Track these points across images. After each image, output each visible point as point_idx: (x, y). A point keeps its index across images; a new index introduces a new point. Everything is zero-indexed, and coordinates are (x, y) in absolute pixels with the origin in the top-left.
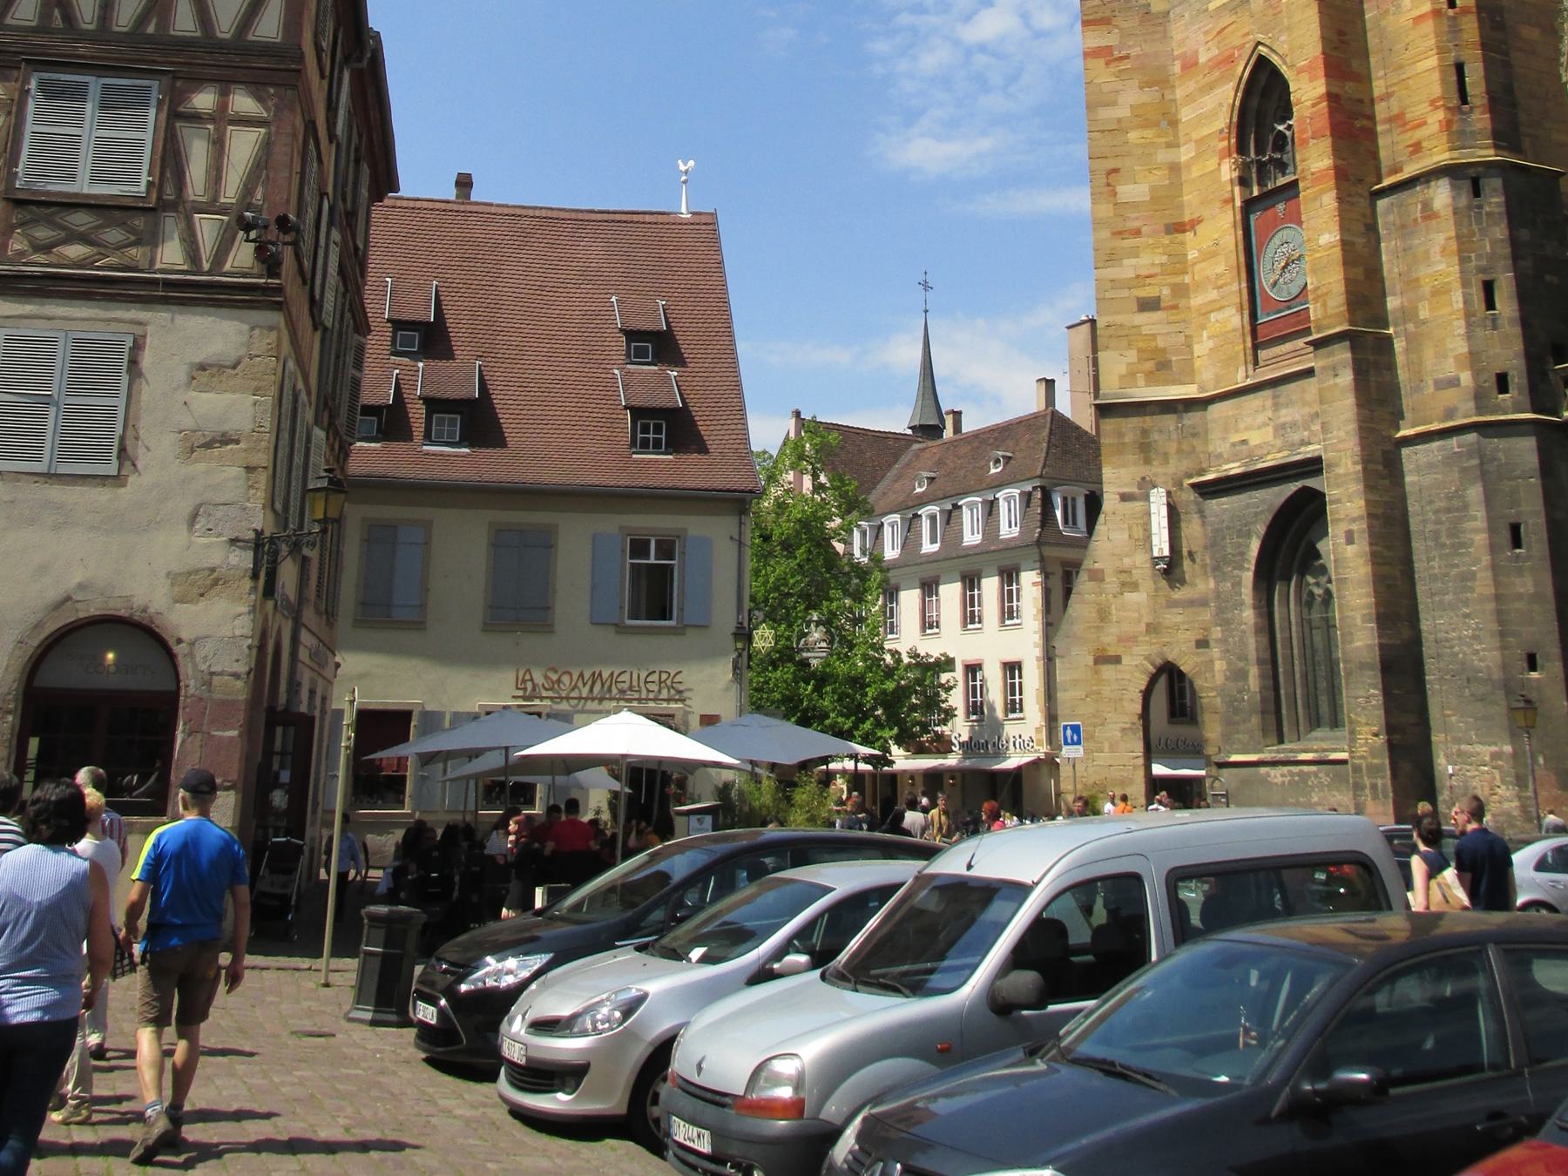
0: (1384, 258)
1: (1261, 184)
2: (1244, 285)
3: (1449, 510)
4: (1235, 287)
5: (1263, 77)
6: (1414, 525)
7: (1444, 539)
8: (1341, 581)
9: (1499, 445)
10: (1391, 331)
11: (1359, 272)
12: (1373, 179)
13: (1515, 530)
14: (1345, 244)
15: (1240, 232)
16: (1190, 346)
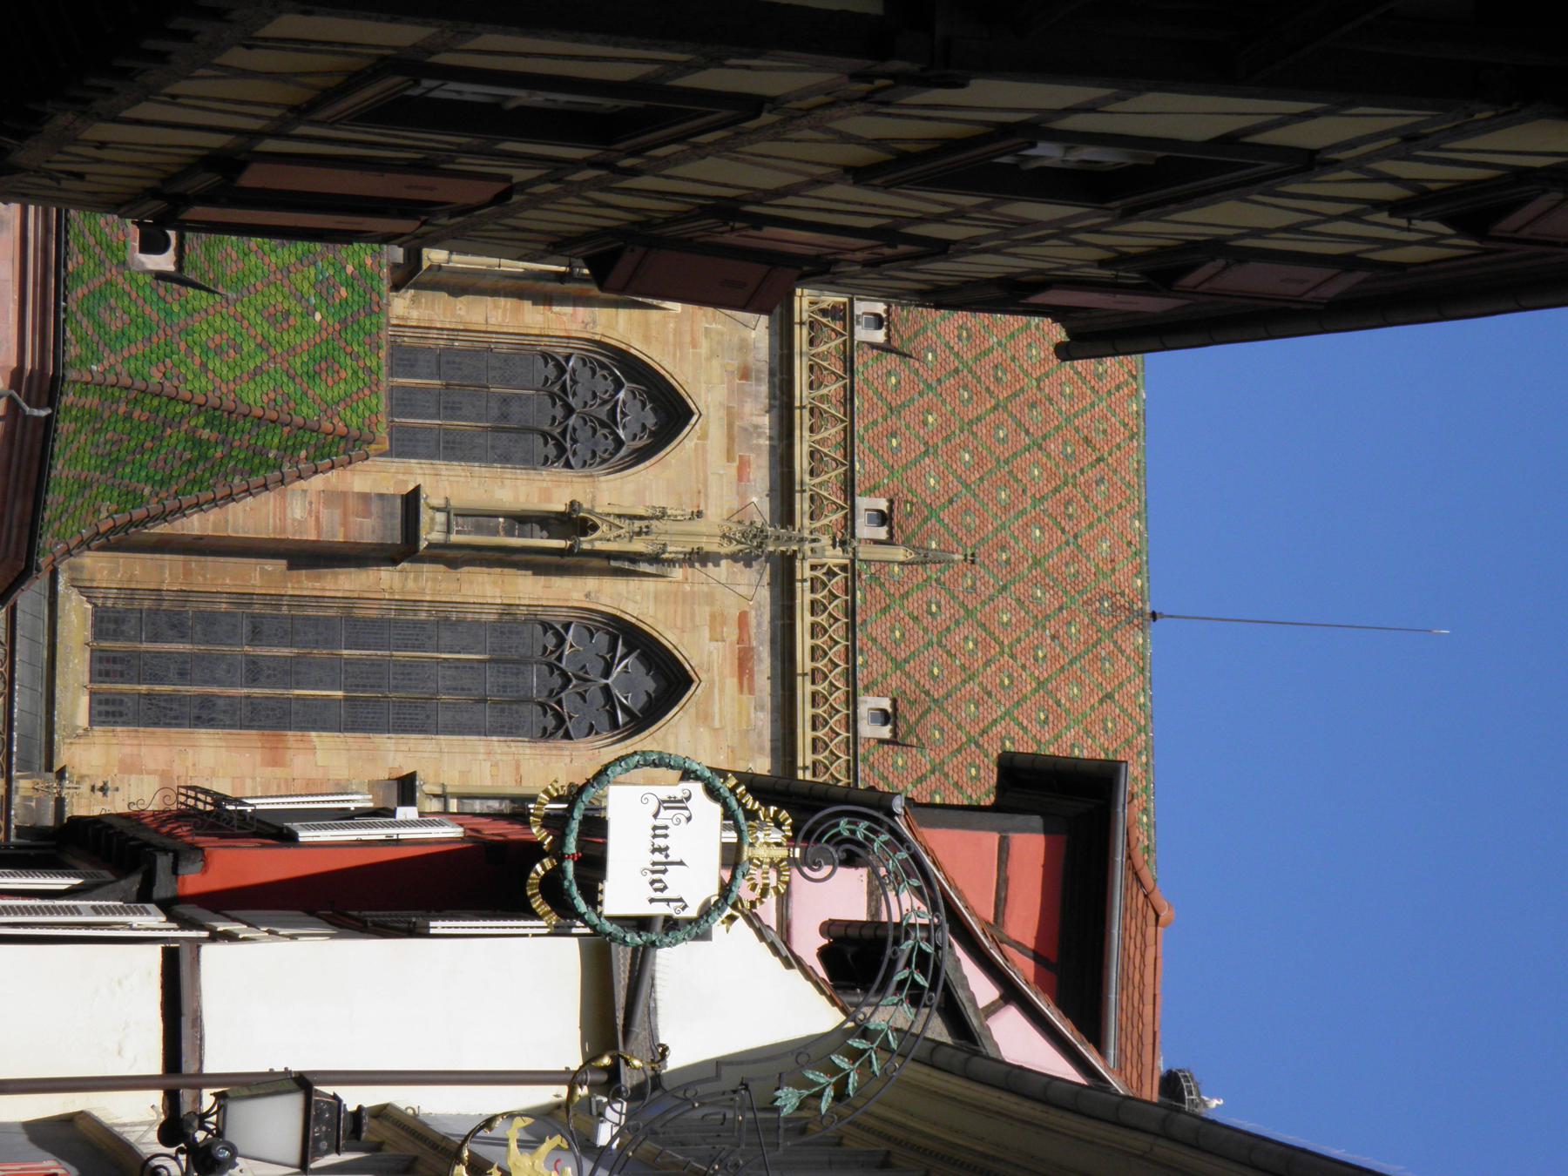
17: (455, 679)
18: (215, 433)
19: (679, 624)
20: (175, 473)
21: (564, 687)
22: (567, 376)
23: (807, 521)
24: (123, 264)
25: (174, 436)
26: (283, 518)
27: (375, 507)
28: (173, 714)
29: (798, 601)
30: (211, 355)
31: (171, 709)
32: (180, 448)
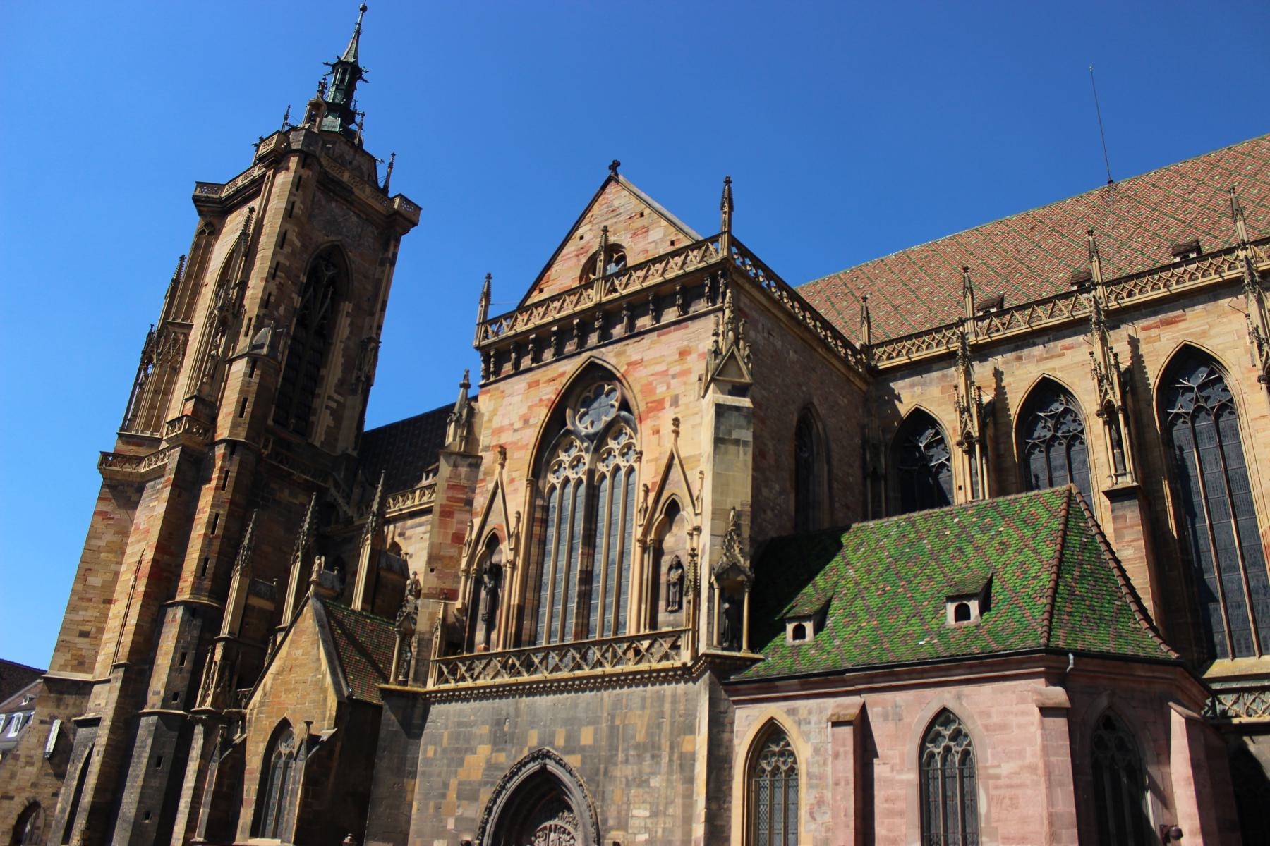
13: (160, 759)
16: (96, 657)
17: (1211, 464)
18: (1076, 568)
19: (1155, 358)
20: (1105, 588)
21: (1203, 408)
22: (1036, 441)
23: (1087, 310)
24: (977, 626)
25: (1080, 589)
26: (1135, 559)
27: (1119, 513)
28: (1265, 609)
29: (1130, 303)
30: (1027, 576)
31: (1263, 610)
32: (1087, 586)
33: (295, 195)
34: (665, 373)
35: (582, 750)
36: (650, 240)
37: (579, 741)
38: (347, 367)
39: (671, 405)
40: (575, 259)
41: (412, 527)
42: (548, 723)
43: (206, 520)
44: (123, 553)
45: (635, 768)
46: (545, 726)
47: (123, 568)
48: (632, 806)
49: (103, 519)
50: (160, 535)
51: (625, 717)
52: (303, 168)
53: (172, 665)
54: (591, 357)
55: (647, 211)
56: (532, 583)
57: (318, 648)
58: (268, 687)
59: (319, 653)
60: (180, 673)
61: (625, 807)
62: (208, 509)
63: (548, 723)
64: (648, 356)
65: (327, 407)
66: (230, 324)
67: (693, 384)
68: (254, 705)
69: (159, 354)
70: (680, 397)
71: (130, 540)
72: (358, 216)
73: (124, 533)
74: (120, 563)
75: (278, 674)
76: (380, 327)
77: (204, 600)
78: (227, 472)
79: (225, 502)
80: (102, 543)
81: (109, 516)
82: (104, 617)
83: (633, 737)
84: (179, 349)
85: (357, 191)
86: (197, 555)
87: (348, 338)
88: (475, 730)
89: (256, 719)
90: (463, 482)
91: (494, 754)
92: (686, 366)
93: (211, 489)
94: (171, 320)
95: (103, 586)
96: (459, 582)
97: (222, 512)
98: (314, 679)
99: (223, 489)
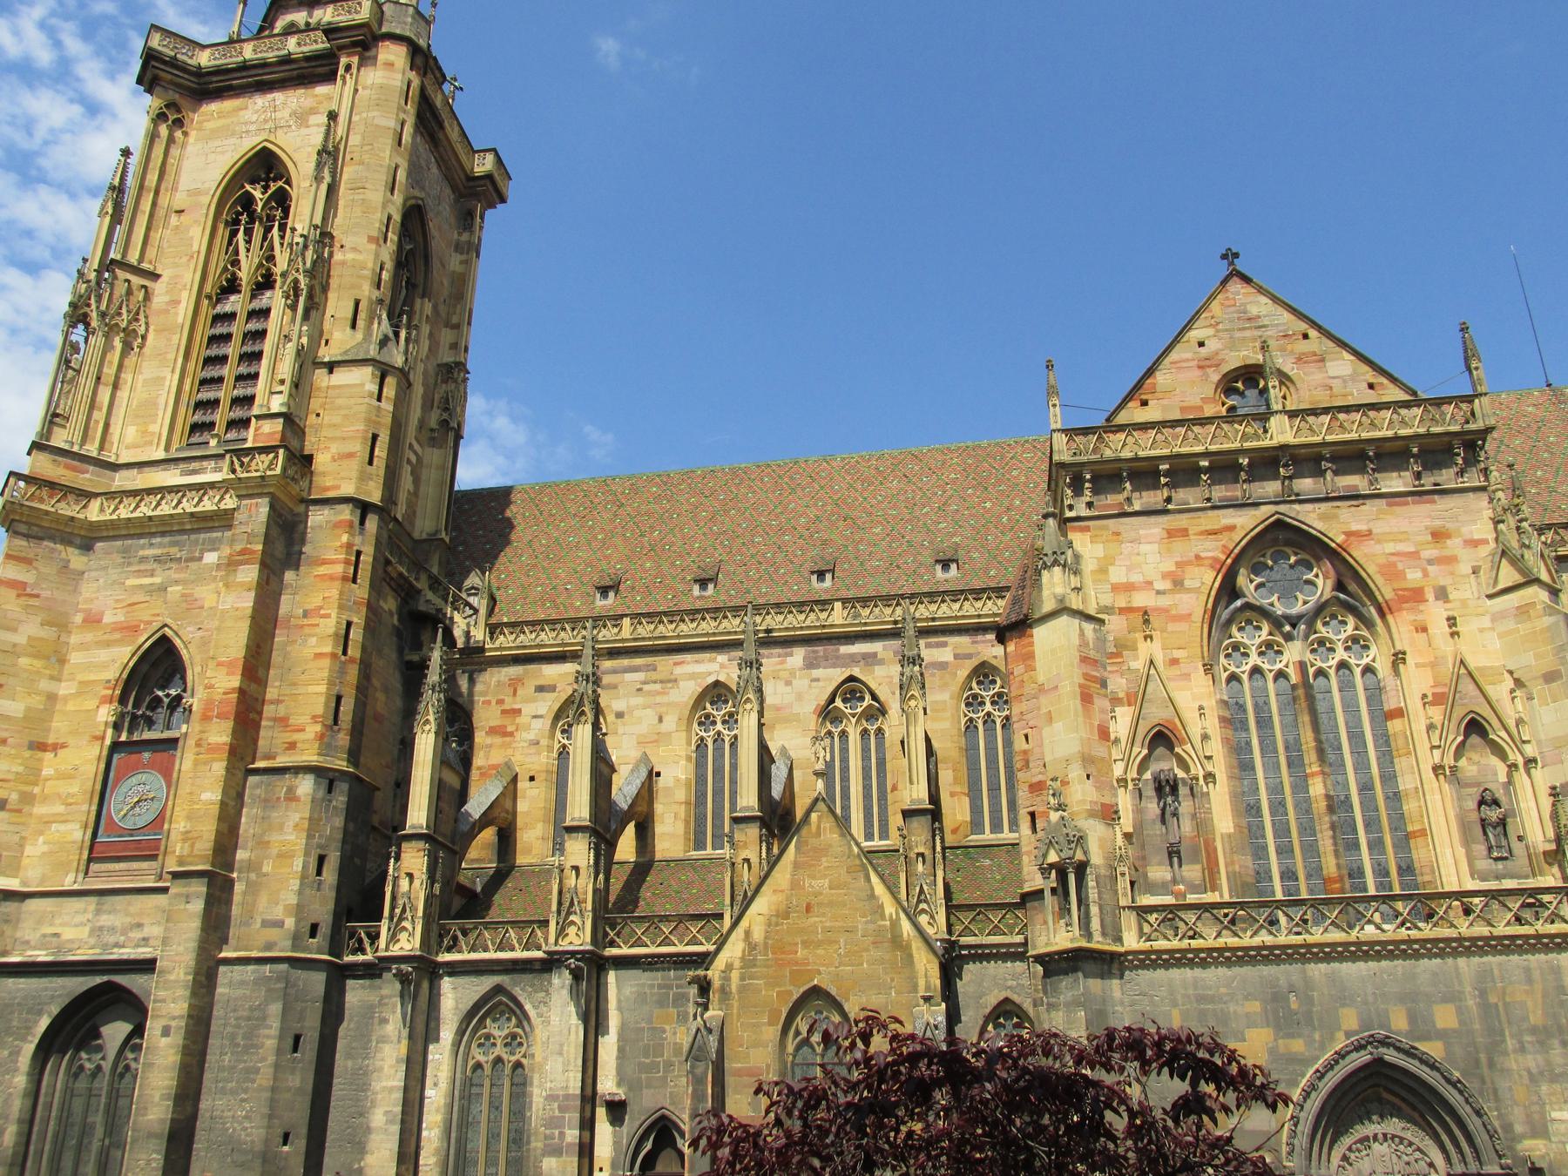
0: (243, 820)
1: (130, 732)
2: (94, 807)
3: (249, 1019)
4: (85, 807)
5: (159, 651)
6: (215, 1026)
7: (239, 1040)
8: (151, 1065)
9: (301, 975)
10: (235, 875)
11: (225, 829)
12: (250, 759)
13: (297, 1038)
14: (223, 804)
15: (102, 766)
16: (22, 846)
33: (405, 112)
34: (1415, 555)
35: (1442, 1035)
36: (1331, 373)
37: (1434, 1026)
38: (428, 404)
39: (1437, 598)
40: (1198, 373)
41: (615, 671)
42: (1370, 999)
43: (332, 631)
44: (62, 661)
45: (1539, 1057)
46: (1365, 1003)
47: (64, 689)
48: (1548, 1107)
49: (19, 596)
50: (248, 646)
51: (1504, 993)
52: (411, 69)
53: (303, 877)
54: (1277, 513)
55: (1313, 333)
56: (1248, 809)
57: (868, 879)
58: (758, 935)
59: (872, 889)
60: (318, 890)
61: (1535, 1108)
62: (334, 615)
63: (1370, 999)
64: (1378, 528)
65: (409, 461)
66: (317, 300)
67: (1468, 576)
68: (729, 967)
69: (103, 315)
70: (1449, 589)
71: (74, 639)
72: (439, 166)
73: (60, 623)
74: (57, 678)
75: (777, 916)
76: (466, 349)
77: (341, 764)
78: (359, 553)
79: (360, 604)
80: (20, 638)
81: (29, 590)
82: (33, 775)
83: (1525, 1018)
84: (137, 313)
85: (446, 124)
86: (323, 688)
87: (427, 357)
88: (1232, 1008)
89: (742, 989)
90: (1092, 654)
91: (1280, 1041)
92: (1447, 552)
93: (332, 578)
94: (112, 255)
95: (24, 717)
96: (1116, 795)
97: (355, 620)
98: (871, 926)
99: (354, 581)
